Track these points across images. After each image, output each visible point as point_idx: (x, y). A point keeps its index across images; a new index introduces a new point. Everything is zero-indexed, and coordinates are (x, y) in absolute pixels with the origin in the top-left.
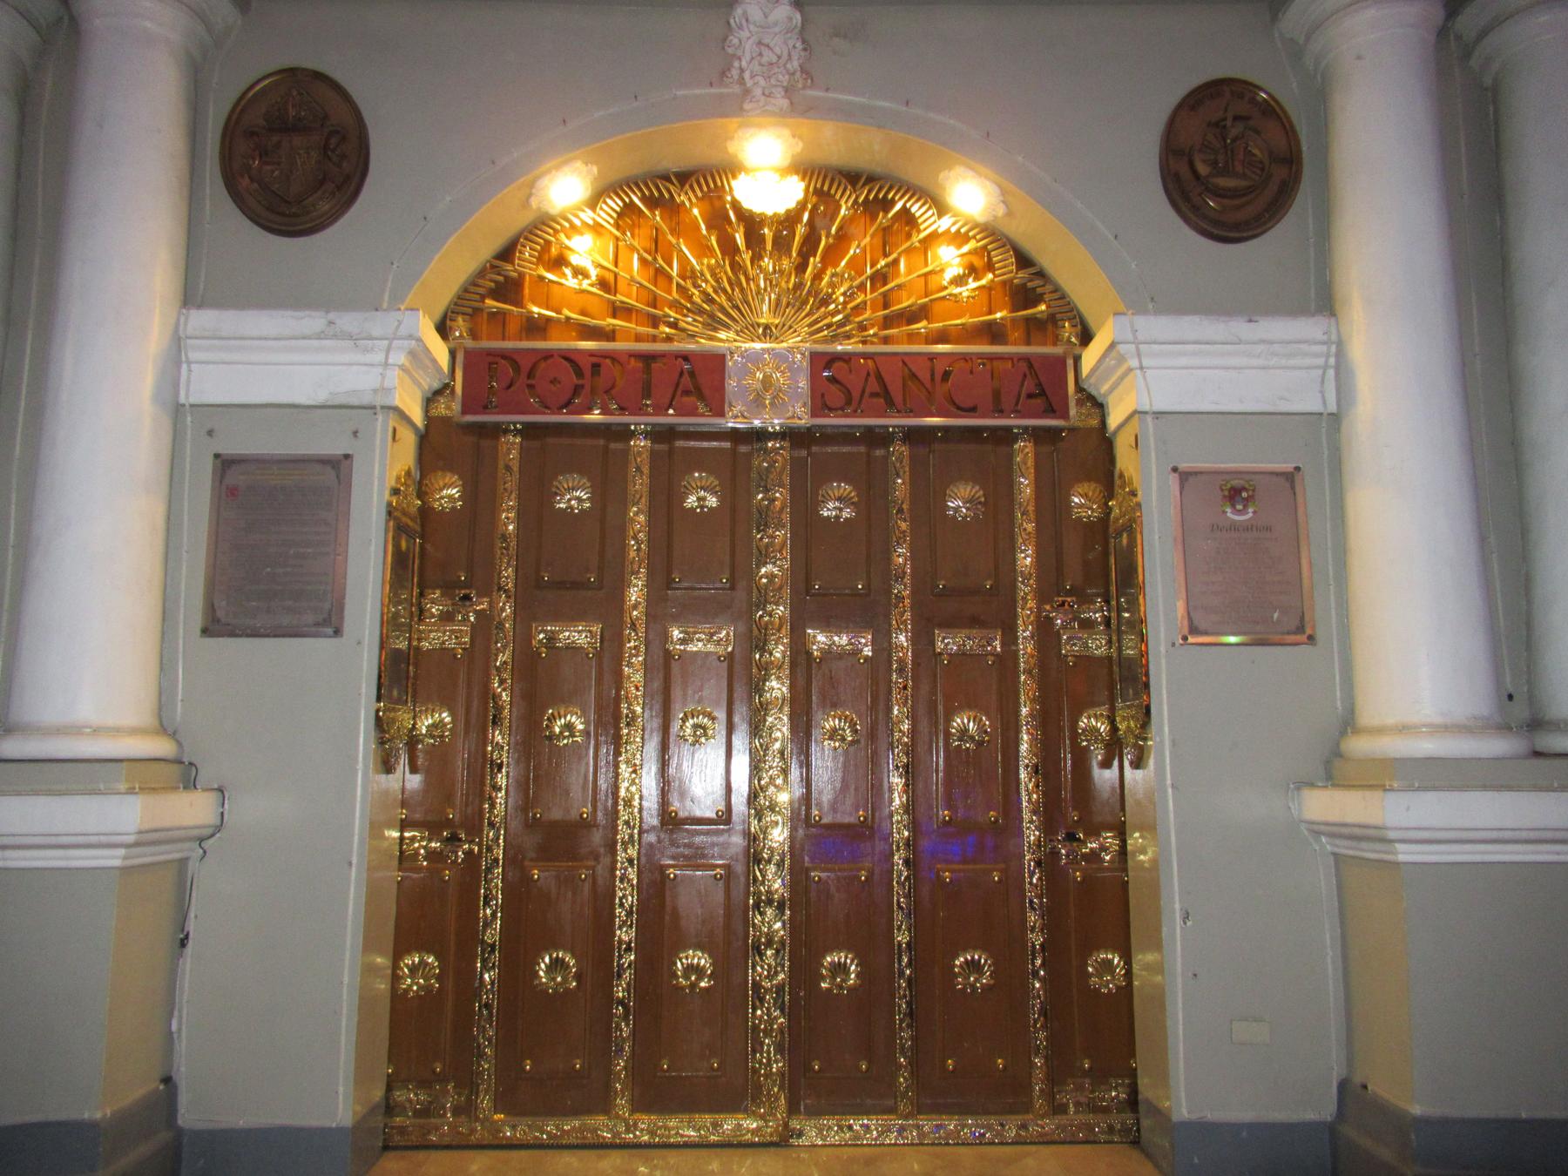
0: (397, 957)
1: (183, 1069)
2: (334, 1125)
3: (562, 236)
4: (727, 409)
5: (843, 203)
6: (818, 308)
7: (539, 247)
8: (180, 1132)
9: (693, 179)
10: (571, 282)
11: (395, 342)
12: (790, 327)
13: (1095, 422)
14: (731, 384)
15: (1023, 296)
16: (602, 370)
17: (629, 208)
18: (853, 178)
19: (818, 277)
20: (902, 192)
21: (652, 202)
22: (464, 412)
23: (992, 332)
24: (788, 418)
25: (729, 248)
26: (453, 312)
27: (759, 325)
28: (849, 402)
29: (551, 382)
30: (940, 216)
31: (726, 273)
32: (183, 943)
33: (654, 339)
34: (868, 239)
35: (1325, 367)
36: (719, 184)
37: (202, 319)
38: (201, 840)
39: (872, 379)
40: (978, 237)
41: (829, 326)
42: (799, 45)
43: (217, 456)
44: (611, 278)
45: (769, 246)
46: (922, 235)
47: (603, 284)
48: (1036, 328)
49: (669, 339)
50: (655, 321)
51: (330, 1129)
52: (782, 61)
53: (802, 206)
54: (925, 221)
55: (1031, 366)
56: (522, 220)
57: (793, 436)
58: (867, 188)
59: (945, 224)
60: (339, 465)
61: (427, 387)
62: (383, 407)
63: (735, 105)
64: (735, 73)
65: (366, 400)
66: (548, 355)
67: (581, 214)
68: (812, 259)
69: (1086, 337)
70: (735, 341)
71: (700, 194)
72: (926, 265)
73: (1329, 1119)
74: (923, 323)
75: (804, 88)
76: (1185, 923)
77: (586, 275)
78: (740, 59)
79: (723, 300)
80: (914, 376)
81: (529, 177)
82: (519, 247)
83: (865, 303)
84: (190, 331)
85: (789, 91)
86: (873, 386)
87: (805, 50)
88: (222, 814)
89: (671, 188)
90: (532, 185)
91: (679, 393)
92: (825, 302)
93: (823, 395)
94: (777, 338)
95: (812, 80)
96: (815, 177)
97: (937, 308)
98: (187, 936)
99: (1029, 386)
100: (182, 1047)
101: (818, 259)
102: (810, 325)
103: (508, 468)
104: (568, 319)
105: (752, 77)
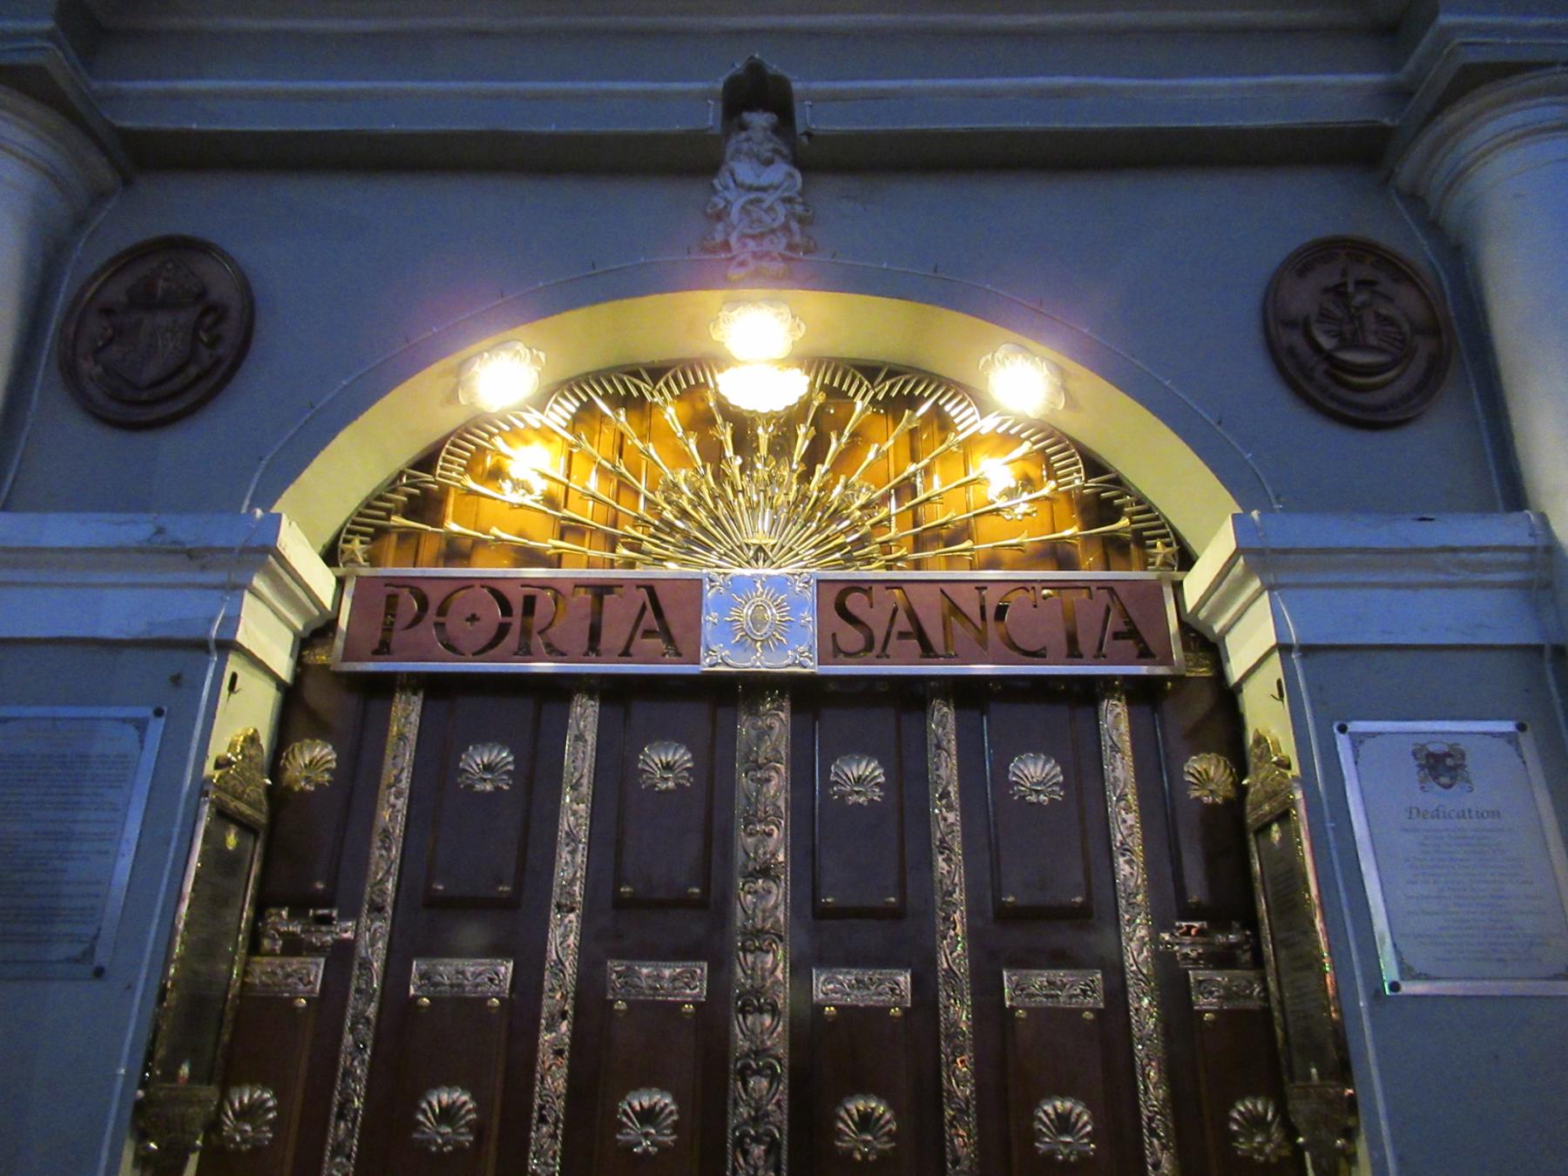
3: (498, 441)
5: (858, 401)
6: (827, 526)
7: (468, 454)
9: (669, 375)
12: (791, 549)
13: (1204, 672)
14: (710, 618)
15: (1097, 510)
17: (587, 408)
18: (871, 371)
19: (826, 488)
21: (616, 401)
22: (346, 658)
23: (1058, 555)
24: (789, 665)
25: (713, 453)
26: (350, 532)
28: (869, 646)
29: (468, 620)
30: (982, 417)
31: (707, 482)
33: (612, 564)
34: (891, 442)
36: (702, 380)
39: (902, 616)
40: (1033, 439)
41: (840, 547)
44: (559, 491)
45: (763, 451)
46: (961, 437)
47: (550, 500)
48: (1114, 550)
49: (630, 564)
50: (612, 542)
53: (805, 404)
54: (962, 422)
56: (450, 419)
58: (888, 384)
59: (988, 425)
61: (300, 627)
66: (467, 584)
67: (525, 415)
69: (1186, 559)
71: (677, 392)
72: (966, 474)
74: (967, 544)
77: (529, 491)
79: (702, 515)
80: (955, 609)
82: (443, 454)
83: (889, 519)
86: (903, 623)
89: (642, 385)
92: (836, 516)
93: (834, 635)
94: (773, 563)
99: (1115, 623)
102: (816, 547)
104: (498, 539)
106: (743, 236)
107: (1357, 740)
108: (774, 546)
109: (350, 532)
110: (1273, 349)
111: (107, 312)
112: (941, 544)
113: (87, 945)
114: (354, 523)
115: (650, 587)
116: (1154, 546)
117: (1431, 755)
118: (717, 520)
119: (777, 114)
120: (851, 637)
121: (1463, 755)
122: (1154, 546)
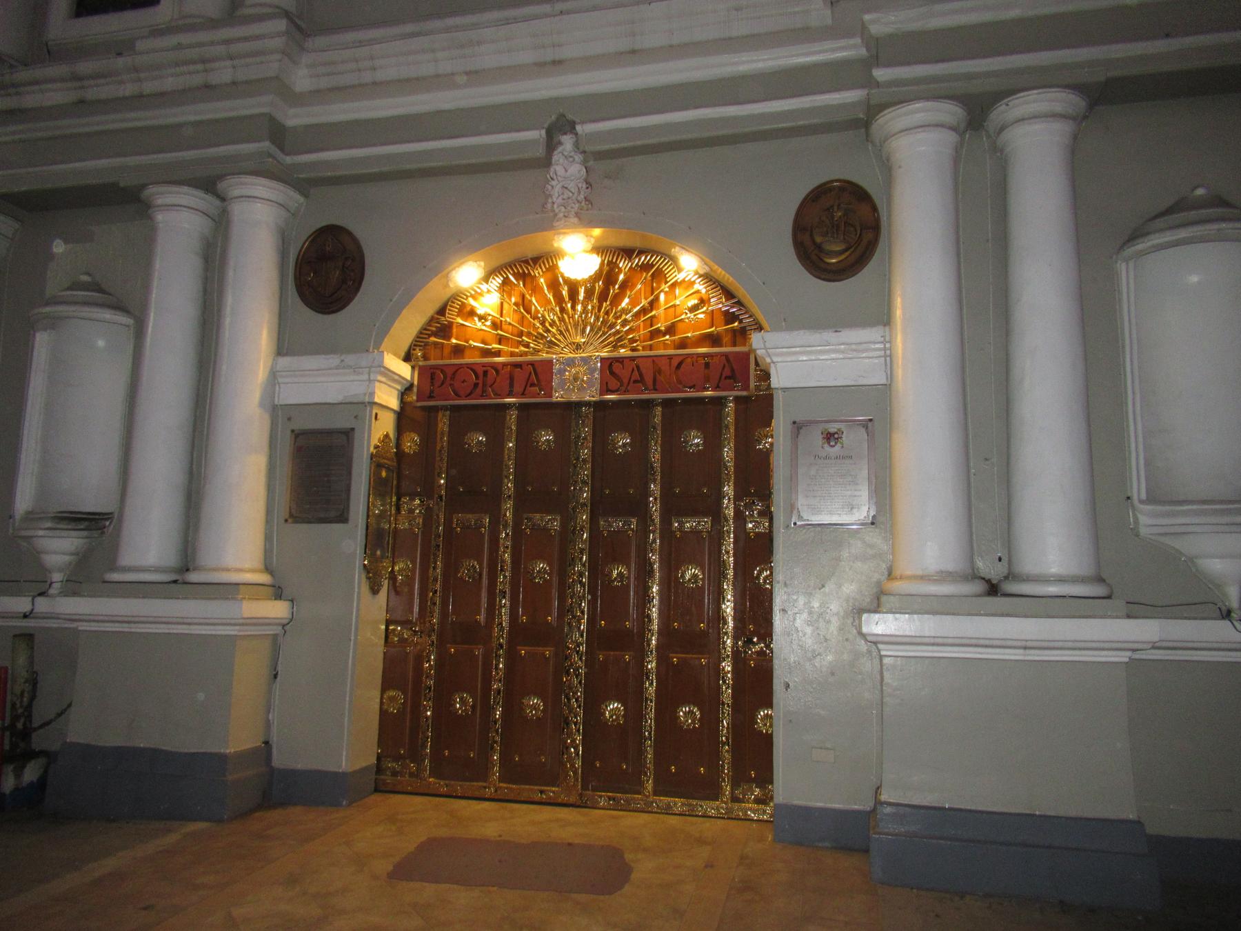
0: (383, 691)
1: (275, 739)
2: (341, 771)
8: (272, 771)
9: (541, 261)
10: (479, 325)
11: (373, 369)
16: (489, 374)
17: (506, 282)
18: (628, 253)
19: (607, 313)
22: (417, 401)
23: (713, 340)
25: (559, 299)
26: (415, 345)
27: (574, 343)
32: (275, 676)
35: (885, 356)
37: (285, 362)
38: (284, 626)
39: (636, 371)
42: (584, 186)
43: (293, 431)
44: (499, 322)
51: (339, 773)
52: (574, 198)
55: (728, 360)
60: (348, 434)
62: (369, 403)
63: (549, 223)
64: (549, 206)
65: (360, 400)
66: (461, 366)
67: (480, 286)
68: (605, 303)
70: (561, 353)
71: (544, 270)
73: (869, 809)
75: (587, 210)
76: (787, 690)
78: (552, 197)
81: (445, 272)
82: (448, 307)
84: (278, 368)
85: (577, 215)
86: (636, 375)
87: (587, 188)
88: (293, 613)
90: (447, 275)
91: (529, 385)
93: (607, 383)
95: (592, 204)
96: (608, 254)
97: (680, 326)
98: (277, 672)
99: (727, 372)
100: (274, 730)
101: (608, 303)
105: (558, 207)
108: (584, 342)
109: (415, 345)
112: (661, 335)
114: (416, 341)
115: (532, 364)
117: (829, 433)
118: (561, 333)
120: (614, 383)
121: (843, 433)
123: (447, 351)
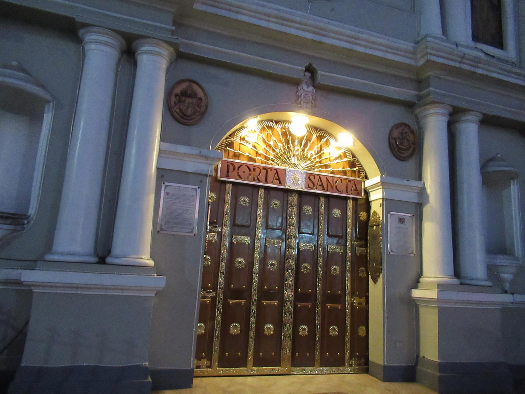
4: (286, 185)
9: (279, 123)
15: (352, 165)
18: (316, 129)
20: (327, 134)
23: (344, 173)
24: (300, 189)
41: (310, 166)
49: (272, 164)
57: (300, 193)
58: (319, 132)
69: (366, 178)
93: (308, 184)
103: (228, 193)
106: (304, 102)
107: (391, 215)
110: (390, 145)
111: (176, 95)
113: (192, 230)
114: (219, 147)
115: (276, 170)
116: (361, 173)
117: (401, 219)
118: (288, 158)
119: (311, 73)
121: (405, 219)
122: (361, 173)
123: (231, 155)
